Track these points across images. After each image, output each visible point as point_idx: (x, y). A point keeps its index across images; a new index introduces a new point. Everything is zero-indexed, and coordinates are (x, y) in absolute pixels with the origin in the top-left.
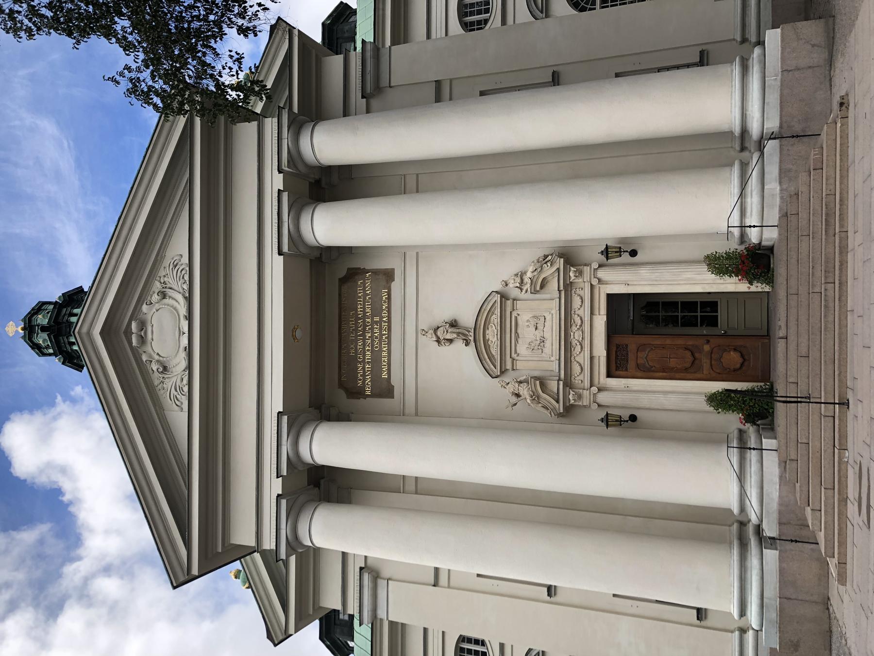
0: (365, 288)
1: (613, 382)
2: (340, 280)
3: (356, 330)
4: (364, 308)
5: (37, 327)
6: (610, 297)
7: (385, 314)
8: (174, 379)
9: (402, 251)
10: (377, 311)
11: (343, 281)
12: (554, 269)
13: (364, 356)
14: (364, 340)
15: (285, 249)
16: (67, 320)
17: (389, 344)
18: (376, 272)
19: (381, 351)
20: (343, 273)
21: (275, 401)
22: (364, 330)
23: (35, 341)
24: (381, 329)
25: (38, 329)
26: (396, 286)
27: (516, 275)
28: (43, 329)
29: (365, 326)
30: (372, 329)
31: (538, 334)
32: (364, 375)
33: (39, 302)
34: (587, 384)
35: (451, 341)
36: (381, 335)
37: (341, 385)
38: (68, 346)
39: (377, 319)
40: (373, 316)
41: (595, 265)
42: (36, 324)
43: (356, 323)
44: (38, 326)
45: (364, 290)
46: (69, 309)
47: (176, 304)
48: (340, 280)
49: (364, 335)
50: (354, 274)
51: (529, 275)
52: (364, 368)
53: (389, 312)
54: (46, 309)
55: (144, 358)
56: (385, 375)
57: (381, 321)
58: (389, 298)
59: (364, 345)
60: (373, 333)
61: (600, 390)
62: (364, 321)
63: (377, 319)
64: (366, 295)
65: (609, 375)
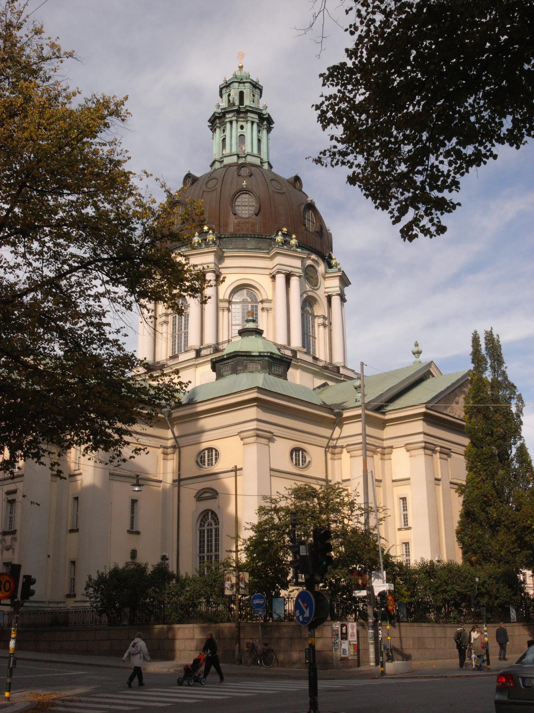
33: (262, 87)
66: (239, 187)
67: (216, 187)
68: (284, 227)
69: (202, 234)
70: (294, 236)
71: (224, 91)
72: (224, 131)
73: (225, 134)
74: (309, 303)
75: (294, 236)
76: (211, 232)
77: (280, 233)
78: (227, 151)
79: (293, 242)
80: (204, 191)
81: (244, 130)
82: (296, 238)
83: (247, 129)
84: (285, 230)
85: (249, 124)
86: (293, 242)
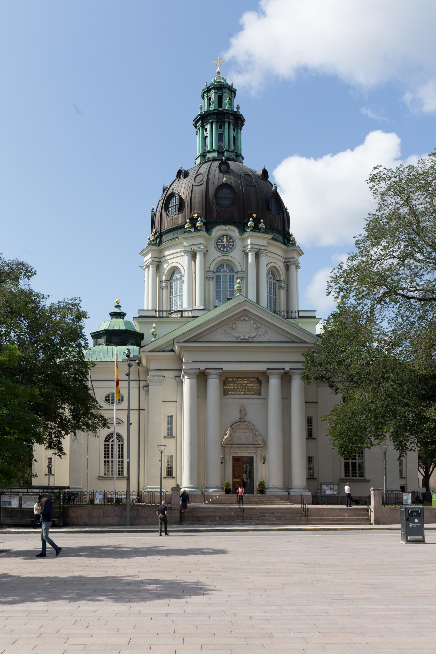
0: (255, 386)
1: (231, 458)
2: (258, 378)
3: (243, 383)
4: (250, 386)
5: (221, 92)
6: (253, 457)
7: (248, 393)
8: (231, 332)
9: (266, 399)
10: (249, 390)
11: (258, 379)
12: (260, 443)
13: (236, 386)
14: (240, 386)
15: (269, 371)
16: (226, 121)
17: (239, 394)
18: (260, 390)
19: (237, 391)
20: (260, 379)
21: (227, 367)
22: (243, 386)
23: (213, 91)
24: (244, 391)
25: (220, 93)
26: (256, 396)
27: (259, 434)
28: (220, 99)
29: (245, 386)
30: (244, 389)
31: (243, 439)
32: (230, 386)
33: (236, 90)
34: (230, 451)
35: (241, 414)
36: (242, 392)
37: (227, 378)
38: (211, 121)
39: (247, 390)
40: (248, 389)
41: (261, 454)
42: (223, 92)
43: (245, 383)
44: (222, 93)
45: (255, 386)
46: (232, 121)
47: (253, 333)
48: (258, 378)
49: (242, 386)
50: (260, 382)
51: (259, 437)
52: (232, 386)
53: (249, 394)
54: (231, 96)
55: (237, 322)
56: (230, 393)
57: (246, 391)
58: (253, 394)
59: (239, 386)
60: (242, 389)
61: (229, 455)
62: (246, 386)
63: (247, 390)
64: (254, 386)
65: (232, 457)
66: (220, 183)
67: (203, 182)
68: (255, 214)
69: (193, 221)
70: (262, 221)
71: (206, 95)
72: (206, 130)
73: (207, 132)
74: (272, 272)
75: (262, 221)
76: (199, 219)
77: (251, 219)
78: (209, 149)
79: (262, 225)
80: (193, 185)
81: (222, 130)
82: (263, 223)
83: (224, 129)
84: (254, 215)
85: (226, 125)
86: (262, 225)
